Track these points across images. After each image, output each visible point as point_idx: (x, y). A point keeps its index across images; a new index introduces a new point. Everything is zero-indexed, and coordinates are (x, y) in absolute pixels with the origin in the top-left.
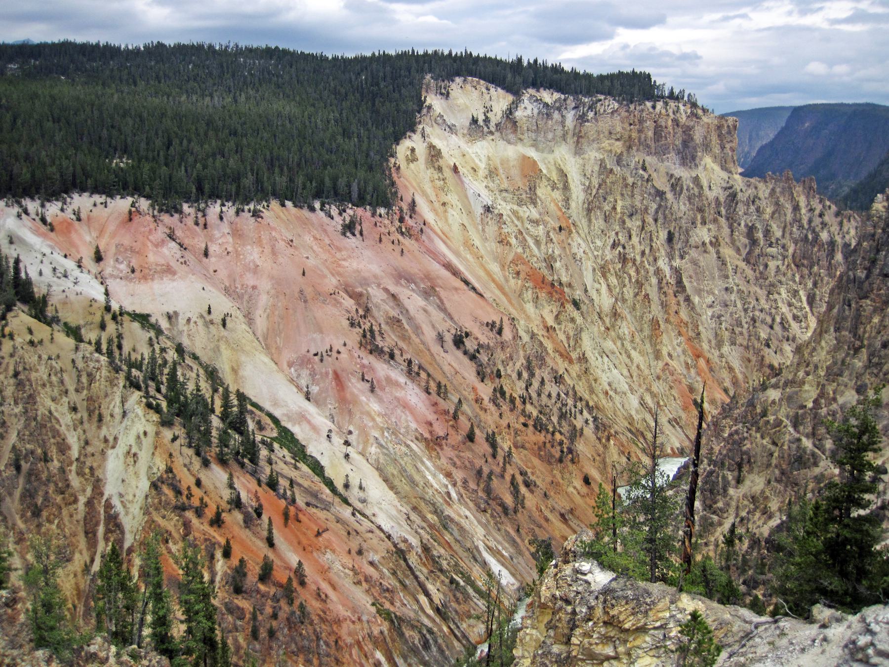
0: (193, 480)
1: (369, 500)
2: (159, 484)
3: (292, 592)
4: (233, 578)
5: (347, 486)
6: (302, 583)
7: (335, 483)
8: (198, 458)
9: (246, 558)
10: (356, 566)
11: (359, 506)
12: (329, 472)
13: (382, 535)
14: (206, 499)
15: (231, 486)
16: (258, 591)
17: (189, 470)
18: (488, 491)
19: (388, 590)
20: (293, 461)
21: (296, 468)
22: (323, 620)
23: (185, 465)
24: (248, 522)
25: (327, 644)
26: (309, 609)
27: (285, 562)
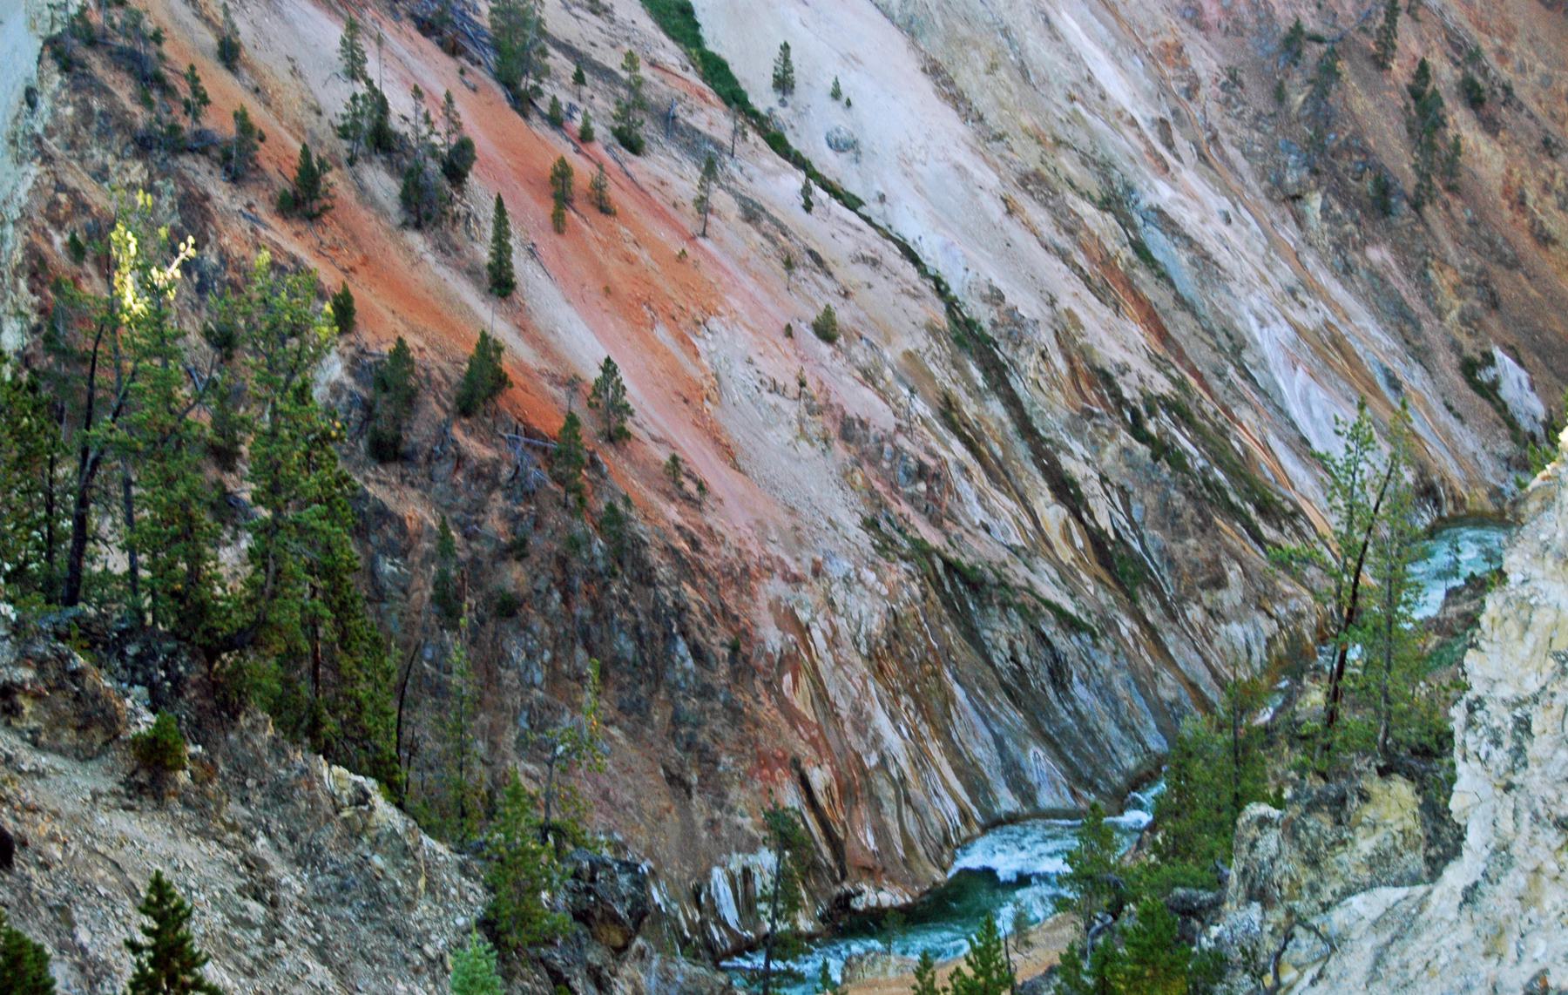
0: (210, 40)
1: (864, 145)
2: (80, 51)
3: (580, 464)
4: (368, 408)
5: (783, 83)
6: (617, 437)
7: (736, 70)
9: (412, 341)
10: (812, 387)
11: (830, 163)
13: (910, 272)
14: (258, 114)
15: (355, 70)
16: (460, 459)
18: (1322, 114)
19: (921, 472)
22: (687, 569)
24: (424, 207)
25: (698, 653)
26: (640, 528)
27: (556, 359)
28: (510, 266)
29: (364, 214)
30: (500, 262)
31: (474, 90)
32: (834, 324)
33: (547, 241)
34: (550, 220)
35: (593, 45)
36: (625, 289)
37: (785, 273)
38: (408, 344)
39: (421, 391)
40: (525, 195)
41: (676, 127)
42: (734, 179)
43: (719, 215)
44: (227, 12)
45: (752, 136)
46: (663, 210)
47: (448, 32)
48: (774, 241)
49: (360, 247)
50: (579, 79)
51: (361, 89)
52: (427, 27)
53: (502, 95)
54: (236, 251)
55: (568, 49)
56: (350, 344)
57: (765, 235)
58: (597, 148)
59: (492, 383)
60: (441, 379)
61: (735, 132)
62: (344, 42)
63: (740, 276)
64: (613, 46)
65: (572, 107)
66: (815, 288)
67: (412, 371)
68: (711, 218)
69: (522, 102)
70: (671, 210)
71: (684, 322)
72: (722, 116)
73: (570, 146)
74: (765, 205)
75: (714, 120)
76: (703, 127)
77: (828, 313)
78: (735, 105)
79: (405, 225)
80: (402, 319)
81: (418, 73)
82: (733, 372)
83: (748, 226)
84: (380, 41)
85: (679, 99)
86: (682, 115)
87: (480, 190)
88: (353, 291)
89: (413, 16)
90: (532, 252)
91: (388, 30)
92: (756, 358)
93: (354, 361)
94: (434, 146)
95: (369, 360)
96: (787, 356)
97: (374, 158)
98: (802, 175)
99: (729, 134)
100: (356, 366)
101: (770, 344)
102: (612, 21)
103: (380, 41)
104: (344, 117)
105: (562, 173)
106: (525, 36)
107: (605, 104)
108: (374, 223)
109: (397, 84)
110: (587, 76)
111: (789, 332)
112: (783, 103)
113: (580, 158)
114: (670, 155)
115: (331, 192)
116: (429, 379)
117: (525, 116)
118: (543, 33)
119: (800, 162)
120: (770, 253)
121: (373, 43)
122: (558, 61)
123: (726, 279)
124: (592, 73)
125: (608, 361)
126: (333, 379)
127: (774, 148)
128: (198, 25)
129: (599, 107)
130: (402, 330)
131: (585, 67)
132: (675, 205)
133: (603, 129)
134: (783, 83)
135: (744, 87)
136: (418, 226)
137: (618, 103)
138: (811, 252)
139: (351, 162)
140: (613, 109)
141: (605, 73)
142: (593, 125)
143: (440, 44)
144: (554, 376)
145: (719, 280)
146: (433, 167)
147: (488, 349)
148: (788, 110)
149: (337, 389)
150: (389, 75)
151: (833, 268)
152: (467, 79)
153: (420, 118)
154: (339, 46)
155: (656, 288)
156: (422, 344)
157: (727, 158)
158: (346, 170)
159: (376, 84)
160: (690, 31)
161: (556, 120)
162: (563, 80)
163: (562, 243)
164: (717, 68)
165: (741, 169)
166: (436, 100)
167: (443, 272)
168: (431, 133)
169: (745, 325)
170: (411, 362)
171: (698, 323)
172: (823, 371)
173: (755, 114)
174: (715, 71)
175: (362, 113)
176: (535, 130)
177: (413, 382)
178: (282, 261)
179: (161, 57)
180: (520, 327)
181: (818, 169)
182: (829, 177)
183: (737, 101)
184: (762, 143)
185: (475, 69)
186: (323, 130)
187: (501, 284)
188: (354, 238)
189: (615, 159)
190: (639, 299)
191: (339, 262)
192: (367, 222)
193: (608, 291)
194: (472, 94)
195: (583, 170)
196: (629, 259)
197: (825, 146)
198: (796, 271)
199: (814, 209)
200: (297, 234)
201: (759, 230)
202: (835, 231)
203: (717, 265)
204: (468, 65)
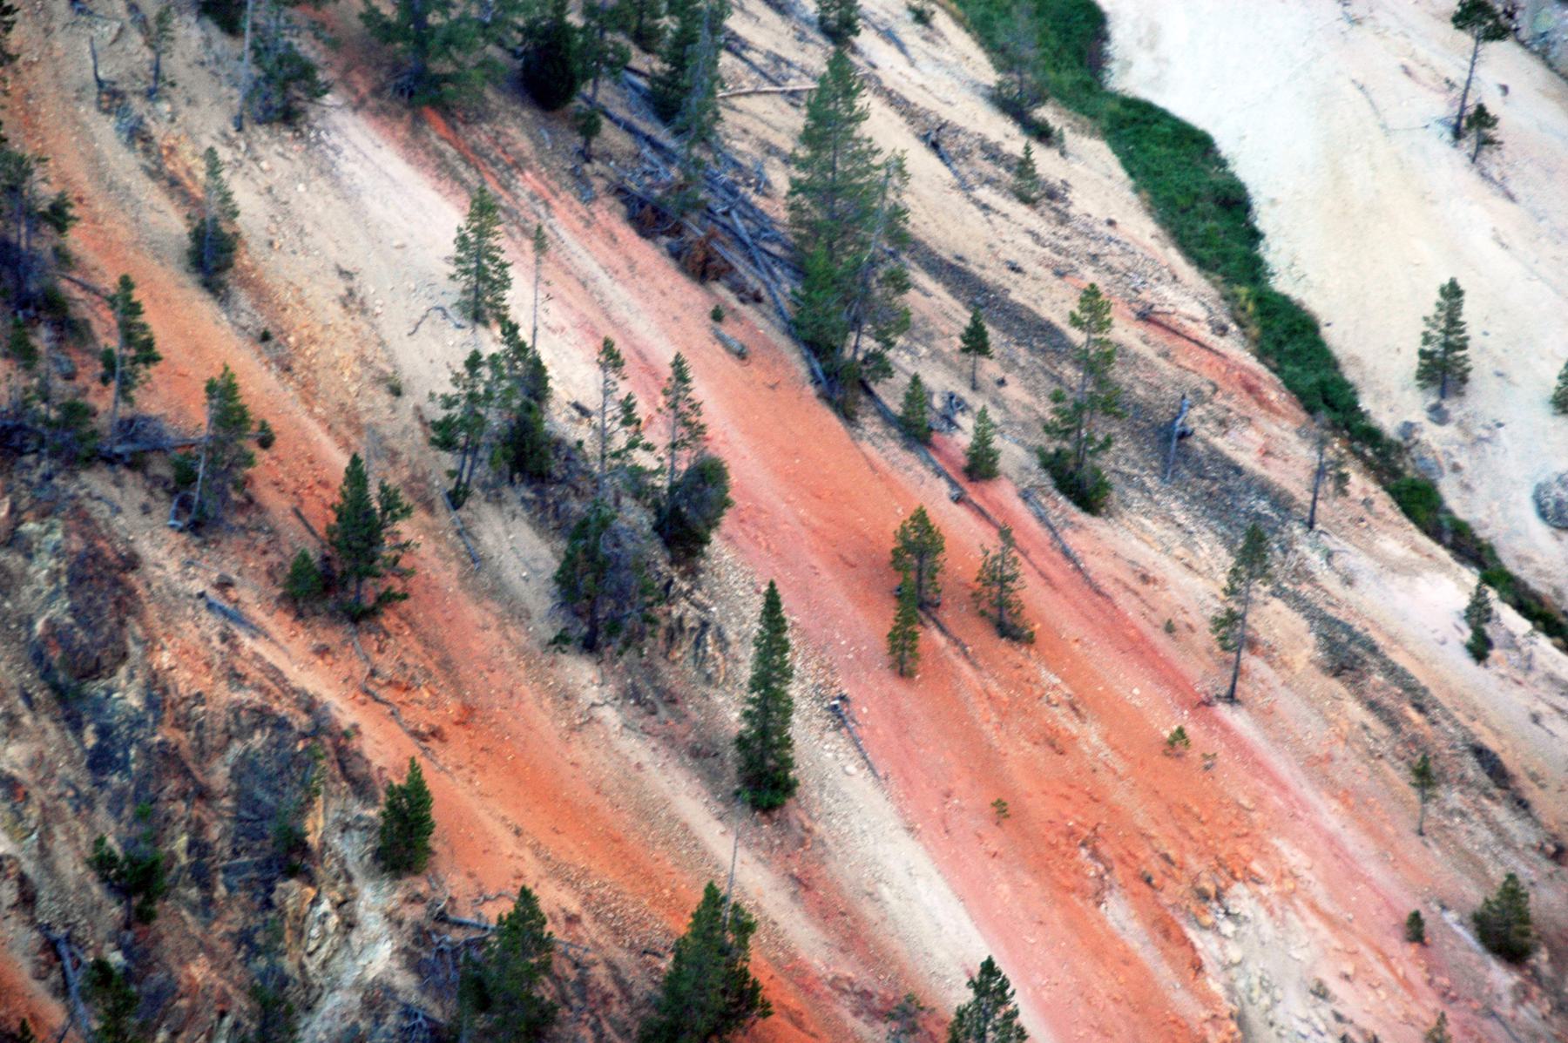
0: (174, 224)
5: (1443, 370)
7: (1338, 337)
8: (222, 42)
9: (553, 898)
12: (1299, 261)
15: (482, 300)
17: (137, 135)
20: (1009, 137)
21: (1029, 188)
23: (111, 97)
28: (787, 743)
29: (473, 613)
30: (764, 733)
31: (741, 355)
32: (1525, 919)
33: (872, 692)
34: (883, 645)
35: (1015, 269)
36: (1040, 808)
37: (1414, 796)
38: (544, 906)
39: (563, 1012)
40: (835, 593)
41: (1186, 456)
42: (1308, 576)
43: (1269, 654)
44: (214, 167)
45: (1360, 483)
46: (1143, 638)
47: (695, 230)
48: (1393, 721)
49: (457, 686)
50: (975, 342)
51: (490, 342)
52: (649, 217)
53: (802, 370)
54: (184, 681)
55: (955, 275)
56: (416, 899)
57: (1373, 706)
58: (1004, 493)
59: (720, 1002)
60: (610, 987)
61: (1320, 473)
62: (462, 242)
63: (1309, 793)
64: (1060, 274)
65: (955, 403)
66: (1484, 834)
67: (545, 967)
68: (1251, 661)
69: (844, 387)
70: (1159, 639)
71: (1173, 892)
72: (1293, 438)
73: (943, 486)
74: (1380, 640)
75: (1271, 443)
76: (1248, 460)
77: (1513, 892)
78: (1324, 416)
79: (561, 641)
80: (536, 849)
81: (620, 313)
82: (1279, 1013)
83: (1336, 685)
84: (540, 242)
85: (1197, 392)
86: (1202, 432)
87: (734, 569)
88: (433, 782)
89: (620, 191)
90: (839, 714)
91: (563, 223)
92: (1335, 986)
93: (422, 936)
94: (638, 473)
95: (457, 936)
96: (1406, 983)
97: (507, 492)
98: (1471, 577)
99: (1306, 476)
100: (425, 947)
101: (1370, 956)
102: (1064, 219)
103: (540, 242)
104: (449, 403)
105: (919, 546)
106: (864, 244)
107: (1027, 399)
108: (493, 636)
109: (574, 335)
110: (994, 335)
111: (1415, 929)
112: (1439, 415)
113: (961, 511)
114: (1168, 518)
115: (404, 563)
116: (582, 984)
117: (848, 416)
118: (902, 240)
119: (1466, 545)
120: (1383, 747)
121: (528, 245)
122: (930, 300)
123: (1276, 800)
124: (1007, 330)
125: (989, 968)
126: (370, 975)
127: (1409, 513)
128: (151, 194)
129: (1013, 405)
130: (533, 873)
131: (990, 315)
132: (1170, 628)
133: (1019, 452)
134: (1443, 370)
135: (1351, 374)
136: (590, 646)
137: (1057, 398)
138: (1480, 752)
139: (456, 499)
140: (1045, 409)
141: (1034, 331)
142: (997, 442)
143: (676, 255)
144: (866, 995)
145: (1259, 800)
146: (635, 517)
147: (720, 926)
148: (1449, 430)
149: (376, 998)
150: (555, 314)
151: (1532, 793)
152: (727, 330)
153: (614, 409)
154: (452, 250)
155: (1114, 810)
156: (574, 907)
157: (1298, 531)
158: (445, 518)
159: (524, 334)
160: (1238, 248)
161: (915, 431)
162: (938, 343)
163: (907, 697)
164: (1292, 332)
165: (1329, 556)
166: (655, 375)
167: (636, 749)
168: (632, 445)
169: (1313, 907)
170: (544, 944)
171: (1204, 896)
172: (1490, 1025)
173: (1372, 436)
174: (1289, 338)
175: (489, 395)
176: (867, 447)
177: (545, 991)
178: (282, 708)
179: (63, 258)
180: (798, 880)
181: (1512, 566)
182: (1537, 585)
183: (1331, 405)
184: (1383, 502)
185: (748, 311)
186: (401, 426)
187: (762, 781)
188: (446, 664)
189: (1041, 518)
190: (1071, 833)
191: (407, 715)
192: (480, 633)
193: (1001, 811)
194: (732, 364)
195: (965, 537)
196: (1056, 744)
197: (1529, 513)
198: (1441, 792)
199: (1495, 653)
200: (322, 651)
201: (1360, 695)
202: (1542, 708)
203: (1259, 767)
204: (732, 300)
